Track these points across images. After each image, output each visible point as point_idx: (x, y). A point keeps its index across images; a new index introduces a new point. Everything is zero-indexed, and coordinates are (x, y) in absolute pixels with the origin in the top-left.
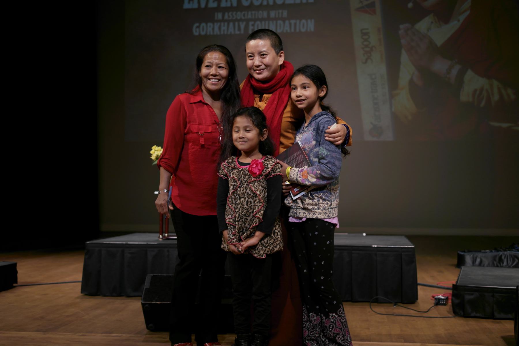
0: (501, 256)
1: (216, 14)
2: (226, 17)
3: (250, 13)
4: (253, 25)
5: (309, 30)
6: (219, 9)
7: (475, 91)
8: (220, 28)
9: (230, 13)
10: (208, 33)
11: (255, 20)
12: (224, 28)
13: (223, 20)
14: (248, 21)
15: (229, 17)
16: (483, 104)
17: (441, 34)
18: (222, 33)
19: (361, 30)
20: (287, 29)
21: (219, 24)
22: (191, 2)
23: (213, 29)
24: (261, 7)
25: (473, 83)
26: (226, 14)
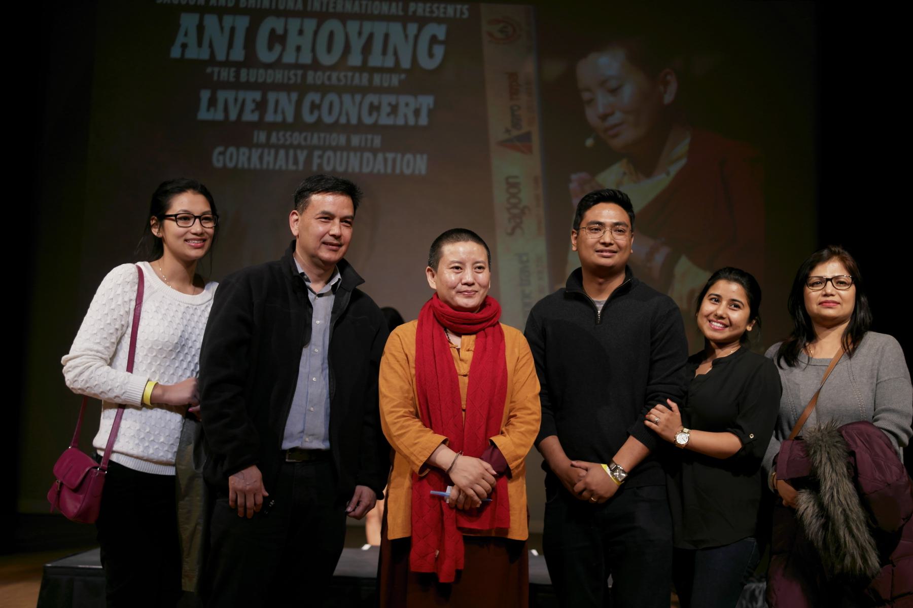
0: (754, 590)
1: (256, 133)
2: (273, 140)
3: (316, 136)
5: (417, 172)
6: (260, 125)
7: (692, 292)
8: (261, 158)
9: (281, 134)
10: (240, 166)
11: (324, 148)
12: (269, 158)
13: (268, 145)
14: (311, 149)
15: (278, 139)
18: (265, 166)
19: (507, 179)
20: (379, 167)
21: (260, 151)
22: (212, 110)
23: (249, 159)
24: (335, 127)
26: (274, 134)
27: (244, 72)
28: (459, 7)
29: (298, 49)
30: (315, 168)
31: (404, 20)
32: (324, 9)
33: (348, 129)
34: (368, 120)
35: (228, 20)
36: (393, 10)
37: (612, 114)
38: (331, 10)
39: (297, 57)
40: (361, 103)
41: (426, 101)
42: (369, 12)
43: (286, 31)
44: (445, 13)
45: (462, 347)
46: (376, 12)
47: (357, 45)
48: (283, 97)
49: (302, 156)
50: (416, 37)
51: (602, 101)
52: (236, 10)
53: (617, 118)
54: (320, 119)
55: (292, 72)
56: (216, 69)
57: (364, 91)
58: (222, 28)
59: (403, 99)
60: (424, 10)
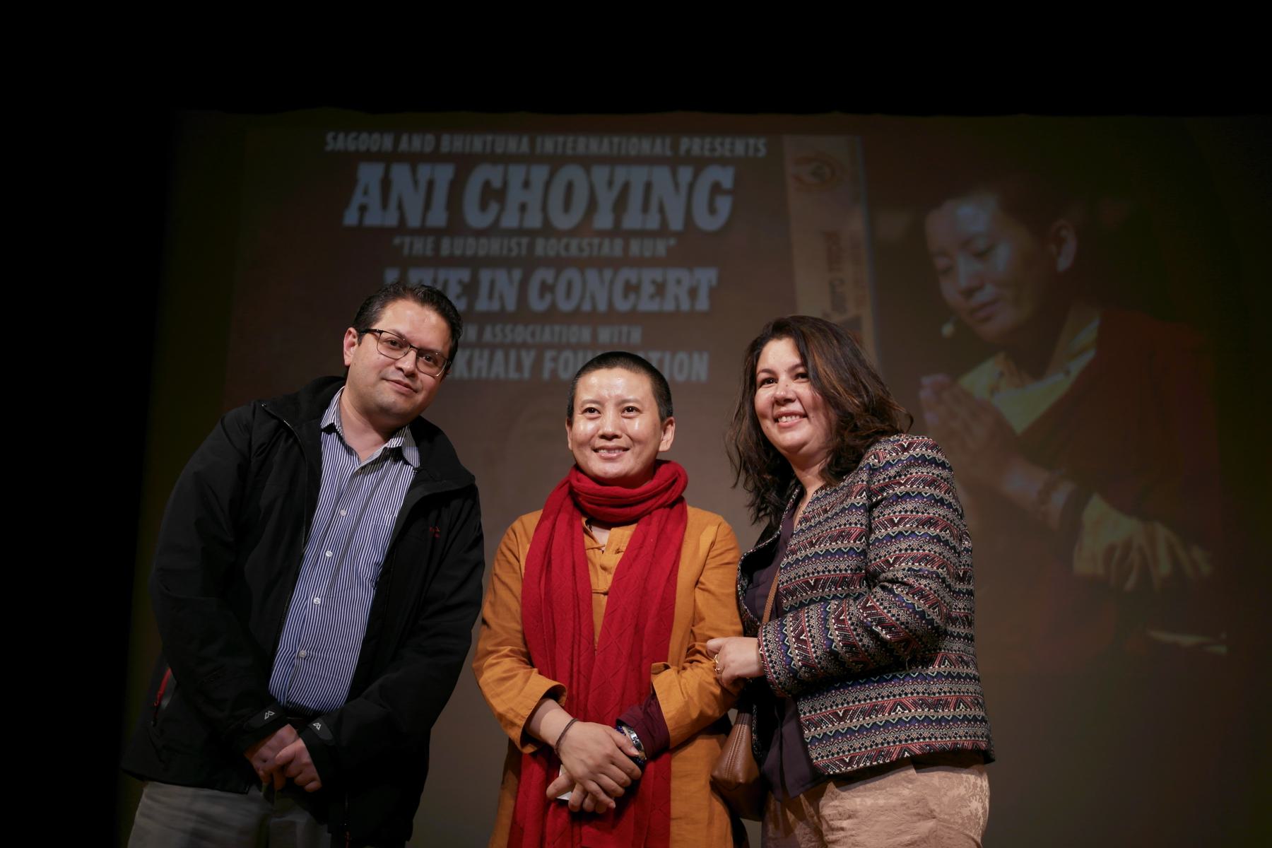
2: (488, 336)
3: (547, 329)
4: (555, 360)
5: (694, 378)
7: (1111, 549)
8: (469, 363)
9: (498, 328)
11: (560, 347)
12: (480, 362)
13: (479, 344)
14: (541, 349)
15: (494, 336)
16: (1130, 584)
17: (1025, 404)
18: (475, 374)
21: (468, 353)
24: (575, 316)
25: (1106, 528)
27: (446, 244)
28: (752, 141)
29: (523, 208)
30: (546, 375)
31: (674, 162)
32: (560, 150)
33: (594, 318)
34: (622, 305)
35: (424, 171)
36: (658, 149)
37: (980, 287)
38: (569, 152)
39: (521, 220)
40: (612, 282)
41: (707, 277)
42: (623, 152)
43: (505, 183)
44: (732, 151)
45: (608, 546)
46: (633, 152)
47: (606, 199)
48: (501, 276)
49: (528, 359)
50: (691, 186)
51: (965, 270)
52: (436, 157)
53: (988, 292)
54: (553, 306)
55: (514, 241)
56: (407, 240)
57: (615, 264)
58: (416, 182)
59: (673, 274)
60: (702, 148)
